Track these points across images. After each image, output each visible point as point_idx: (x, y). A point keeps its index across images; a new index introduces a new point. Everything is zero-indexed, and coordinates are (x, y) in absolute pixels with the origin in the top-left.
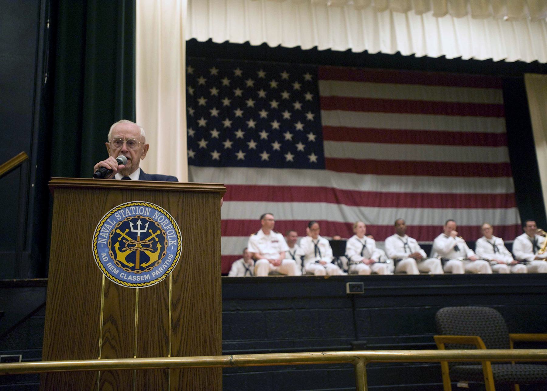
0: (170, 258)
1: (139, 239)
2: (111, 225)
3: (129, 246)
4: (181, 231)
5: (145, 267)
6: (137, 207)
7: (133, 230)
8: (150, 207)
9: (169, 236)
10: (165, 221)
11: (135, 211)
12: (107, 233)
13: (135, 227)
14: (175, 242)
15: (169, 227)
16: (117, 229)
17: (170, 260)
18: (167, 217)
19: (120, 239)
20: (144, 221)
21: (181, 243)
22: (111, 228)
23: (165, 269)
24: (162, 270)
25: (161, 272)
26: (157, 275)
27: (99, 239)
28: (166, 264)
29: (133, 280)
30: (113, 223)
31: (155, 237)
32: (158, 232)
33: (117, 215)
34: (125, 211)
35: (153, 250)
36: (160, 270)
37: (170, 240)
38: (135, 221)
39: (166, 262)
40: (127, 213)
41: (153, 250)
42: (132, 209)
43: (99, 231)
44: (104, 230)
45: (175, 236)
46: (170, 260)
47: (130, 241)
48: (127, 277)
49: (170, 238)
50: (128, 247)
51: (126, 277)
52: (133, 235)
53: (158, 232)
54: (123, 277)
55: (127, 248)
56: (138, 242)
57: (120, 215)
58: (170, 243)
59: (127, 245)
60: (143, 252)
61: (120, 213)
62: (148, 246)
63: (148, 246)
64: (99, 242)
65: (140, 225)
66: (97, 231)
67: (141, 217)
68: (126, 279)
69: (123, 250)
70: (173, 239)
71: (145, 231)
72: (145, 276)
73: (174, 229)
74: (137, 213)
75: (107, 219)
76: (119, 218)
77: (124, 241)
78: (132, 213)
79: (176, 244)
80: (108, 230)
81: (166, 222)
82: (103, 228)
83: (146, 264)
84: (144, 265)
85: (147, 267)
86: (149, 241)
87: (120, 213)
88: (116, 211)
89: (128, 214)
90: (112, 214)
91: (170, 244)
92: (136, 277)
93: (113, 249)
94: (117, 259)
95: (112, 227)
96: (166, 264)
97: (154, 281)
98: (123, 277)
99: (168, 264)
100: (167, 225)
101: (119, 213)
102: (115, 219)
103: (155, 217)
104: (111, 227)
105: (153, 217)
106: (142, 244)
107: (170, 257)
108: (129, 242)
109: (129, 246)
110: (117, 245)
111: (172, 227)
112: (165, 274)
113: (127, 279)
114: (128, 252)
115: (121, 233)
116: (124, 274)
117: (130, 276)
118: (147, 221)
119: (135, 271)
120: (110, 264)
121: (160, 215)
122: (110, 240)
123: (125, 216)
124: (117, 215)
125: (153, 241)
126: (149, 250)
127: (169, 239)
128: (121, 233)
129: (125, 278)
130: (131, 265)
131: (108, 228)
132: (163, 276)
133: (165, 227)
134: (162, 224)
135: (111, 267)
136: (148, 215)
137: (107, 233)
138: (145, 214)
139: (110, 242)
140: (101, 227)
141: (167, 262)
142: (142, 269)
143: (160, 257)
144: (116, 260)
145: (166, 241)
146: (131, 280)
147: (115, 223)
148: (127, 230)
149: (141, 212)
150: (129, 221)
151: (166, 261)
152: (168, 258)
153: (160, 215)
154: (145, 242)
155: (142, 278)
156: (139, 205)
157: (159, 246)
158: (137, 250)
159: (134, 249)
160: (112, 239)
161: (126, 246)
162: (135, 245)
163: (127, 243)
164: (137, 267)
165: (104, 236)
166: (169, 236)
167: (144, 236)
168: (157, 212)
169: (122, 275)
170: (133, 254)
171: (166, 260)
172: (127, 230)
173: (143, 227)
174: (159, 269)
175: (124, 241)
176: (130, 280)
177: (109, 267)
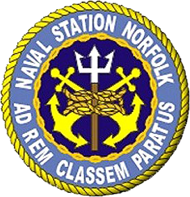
1: (95, 88)
7: (82, 70)
19: (59, 88)
31: (129, 84)
32: (136, 73)
52: (83, 80)
71: (107, 70)
84: (110, 142)
110: (54, 102)
130: (80, 142)
142: (105, 151)
148: (71, 70)
157: (137, 102)
164: (95, 148)
167: (106, 81)
172: (71, 70)
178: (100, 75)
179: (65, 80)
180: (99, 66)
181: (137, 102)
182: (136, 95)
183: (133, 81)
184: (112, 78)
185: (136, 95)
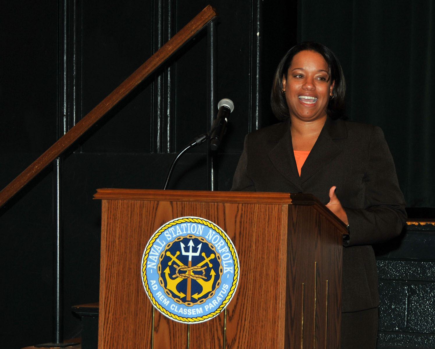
0: (225, 289)
1: (190, 264)
2: (161, 246)
3: (181, 272)
4: (238, 255)
5: (197, 299)
6: (189, 224)
7: (184, 253)
8: (203, 224)
9: (225, 261)
10: (220, 242)
11: (187, 230)
12: (156, 256)
13: (187, 249)
14: (231, 270)
15: (225, 250)
16: (167, 251)
17: (224, 291)
18: (222, 236)
19: (170, 263)
20: (197, 242)
21: (238, 270)
22: (161, 249)
23: (219, 302)
24: (216, 304)
25: (215, 305)
26: (210, 308)
27: (148, 263)
28: (220, 297)
29: (184, 313)
30: (163, 243)
31: (209, 263)
32: (212, 256)
33: (167, 234)
34: (175, 229)
35: (206, 278)
36: (214, 304)
37: (226, 267)
38: (186, 241)
39: (220, 294)
40: (178, 232)
41: (206, 278)
42: (183, 226)
43: (148, 253)
44: (153, 252)
45: (231, 261)
46: (224, 291)
47: (181, 266)
48: (178, 309)
49: (226, 264)
50: (179, 274)
51: (177, 310)
52: (184, 259)
53: (212, 256)
54: (173, 309)
55: (178, 275)
56: (189, 267)
57: (170, 234)
58: (226, 270)
59: (178, 271)
60: (195, 280)
61: (170, 232)
62: (200, 273)
63: (200, 273)
64: (148, 266)
65: (193, 246)
66: (146, 254)
67: (193, 237)
68: (177, 311)
69: (174, 276)
70: (229, 265)
71: (197, 254)
72: (197, 309)
73: (230, 253)
74: (189, 232)
75: (156, 239)
76: (169, 237)
77: (175, 266)
78: (184, 232)
79: (232, 272)
80: (158, 252)
81: (222, 243)
82: (152, 249)
83: (198, 294)
84: (196, 296)
85: (199, 299)
86: (202, 267)
87: (170, 232)
88: (165, 229)
89: (179, 233)
90: (162, 232)
91: (225, 272)
92: (187, 310)
93: (163, 275)
94: (167, 288)
95: (162, 249)
96: (220, 297)
97: (207, 315)
98: (173, 309)
99: (222, 296)
100: (222, 247)
101: (169, 232)
102: (165, 239)
103: (209, 237)
104: (161, 248)
105: (207, 237)
106: (193, 271)
107: (224, 287)
108: (180, 267)
109: (181, 272)
110: (167, 271)
111: (228, 250)
112: (219, 308)
113: (178, 311)
114: (179, 280)
115: (171, 256)
116: (175, 306)
117: (181, 309)
118: (200, 242)
119: (186, 303)
120: (160, 294)
121: (214, 235)
122: (160, 265)
123: (176, 236)
124: (167, 234)
125: (206, 267)
126: (202, 278)
127: (225, 265)
128: (171, 256)
129: (176, 310)
130: (182, 295)
131: (157, 249)
132: (216, 310)
133: (220, 249)
134: (216, 246)
135: (160, 296)
136: (201, 234)
137: (156, 256)
138: (198, 233)
139: (159, 267)
140: (150, 248)
141: (222, 294)
142: (194, 301)
143: (214, 287)
144: (166, 289)
145: (220, 267)
146: (182, 313)
147: (165, 243)
148: (178, 253)
149: (194, 230)
150: (180, 241)
151: (220, 293)
152: (223, 289)
153: (214, 235)
154: (197, 268)
155: (193, 312)
156: (191, 222)
157: (213, 273)
158: (188, 277)
159: (185, 277)
160: (162, 263)
161: (177, 272)
162: (186, 271)
163: (178, 269)
164: (189, 298)
165: (154, 259)
166: (225, 261)
167: (197, 260)
168: (211, 231)
169: (173, 307)
170: (185, 282)
171: (220, 292)
172: (178, 253)
173: (195, 250)
174: (213, 302)
175: (175, 266)
176: (180, 313)
177: (158, 297)
178: (193, 257)
179: (174, 258)
180: (193, 252)
181: (213, 273)
182: (212, 270)
183: (211, 261)
184: (200, 259)
185: (212, 270)
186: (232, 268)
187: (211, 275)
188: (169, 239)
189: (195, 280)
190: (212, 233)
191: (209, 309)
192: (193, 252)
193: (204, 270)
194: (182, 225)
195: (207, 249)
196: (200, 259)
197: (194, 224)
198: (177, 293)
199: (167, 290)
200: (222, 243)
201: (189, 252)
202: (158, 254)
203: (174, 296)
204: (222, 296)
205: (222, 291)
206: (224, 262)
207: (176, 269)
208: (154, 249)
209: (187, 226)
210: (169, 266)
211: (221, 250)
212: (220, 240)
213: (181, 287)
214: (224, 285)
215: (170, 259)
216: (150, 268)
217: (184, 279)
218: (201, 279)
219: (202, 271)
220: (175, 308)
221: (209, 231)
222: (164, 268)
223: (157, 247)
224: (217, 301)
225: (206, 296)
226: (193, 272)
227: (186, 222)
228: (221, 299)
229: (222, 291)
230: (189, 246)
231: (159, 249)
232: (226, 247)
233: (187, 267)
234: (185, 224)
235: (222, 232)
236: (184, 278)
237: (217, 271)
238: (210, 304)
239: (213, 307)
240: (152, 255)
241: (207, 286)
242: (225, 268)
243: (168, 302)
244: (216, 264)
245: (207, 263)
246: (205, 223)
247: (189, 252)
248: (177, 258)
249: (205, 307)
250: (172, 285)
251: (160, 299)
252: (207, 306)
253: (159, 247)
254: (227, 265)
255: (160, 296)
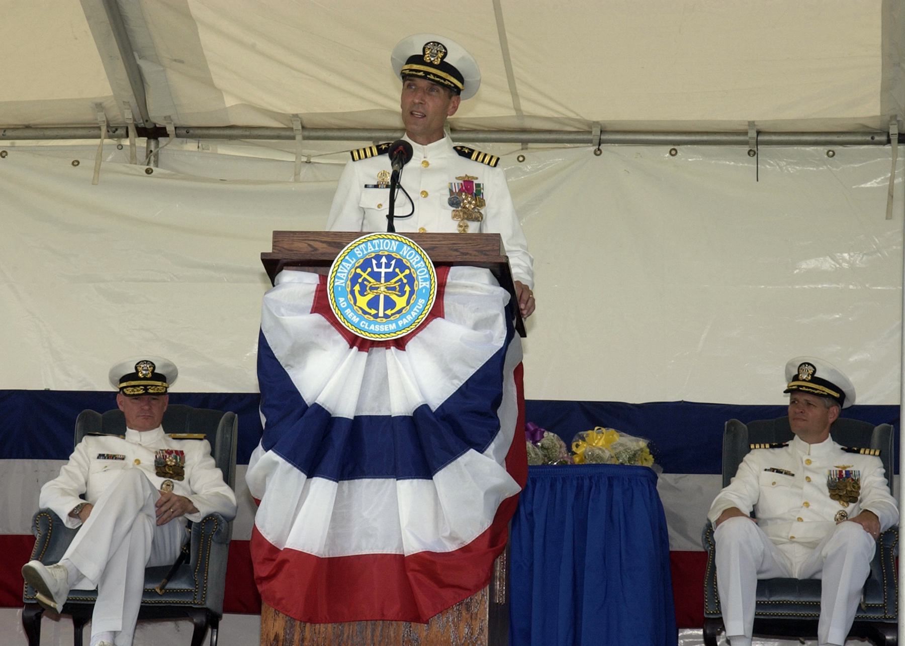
0: (421, 303)
1: (383, 280)
2: (350, 263)
3: (372, 288)
6: (381, 241)
7: (376, 269)
9: (421, 276)
10: (416, 257)
11: (379, 246)
12: (345, 273)
13: (379, 265)
14: (427, 284)
17: (420, 306)
19: (360, 280)
20: (389, 258)
27: (336, 280)
28: (415, 311)
30: (353, 260)
31: (403, 278)
33: (357, 251)
34: (367, 245)
35: (400, 294)
37: (422, 282)
38: (378, 257)
39: (415, 309)
40: (369, 248)
41: (400, 294)
44: (341, 269)
45: (427, 276)
46: (420, 306)
48: (369, 326)
49: (421, 279)
52: (376, 276)
55: (369, 291)
58: (422, 285)
62: (394, 289)
63: (394, 289)
64: (336, 284)
68: (367, 328)
70: (425, 280)
71: (391, 270)
76: (360, 254)
77: (365, 283)
79: (428, 286)
80: (346, 269)
81: (417, 259)
82: (341, 267)
84: (389, 312)
85: (393, 315)
90: (352, 249)
96: (415, 311)
98: (363, 326)
100: (417, 263)
101: (359, 248)
103: (403, 252)
107: (421, 302)
108: (371, 284)
109: (372, 288)
110: (357, 288)
111: (424, 265)
114: (370, 296)
115: (362, 273)
116: (365, 323)
117: (373, 325)
118: (394, 258)
121: (409, 251)
125: (400, 283)
127: (420, 280)
128: (362, 273)
129: (366, 327)
130: (373, 312)
131: (347, 267)
133: (416, 265)
135: (349, 314)
137: (345, 273)
138: (391, 249)
141: (417, 308)
143: (408, 302)
144: (356, 306)
148: (369, 270)
152: (418, 304)
153: (409, 251)
157: (407, 288)
159: (377, 293)
161: (368, 288)
162: (378, 288)
164: (381, 314)
165: (342, 277)
166: (421, 276)
167: (389, 277)
168: (405, 247)
169: (363, 324)
172: (369, 270)
175: (365, 283)
176: (372, 330)
177: (347, 314)
179: (365, 275)
180: (386, 268)
181: (407, 288)
184: (394, 274)
186: (428, 283)
187: (406, 291)
188: (359, 256)
189: (388, 296)
190: (407, 249)
191: (403, 324)
192: (386, 268)
193: (399, 285)
194: (374, 241)
195: (401, 265)
196: (394, 274)
197: (388, 241)
198: (367, 310)
199: (357, 307)
200: (417, 259)
201: (381, 268)
202: (346, 271)
203: (365, 312)
204: (418, 311)
205: (417, 306)
206: (420, 277)
207: (367, 286)
208: (343, 266)
209: (380, 242)
210: (360, 284)
211: (417, 265)
212: (415, 256)
213: (373, 303)
214: (420, 299)
215: (361, 276)
216: (338, 286)
217: (376, 296)
218: (395, 295)
219: (395, 287)
220: (365, 325)
221: (404, 247)
222: (353, 285)
223: (346, 264)
224: (412, 316)
225: (400, 311)
226: (386, 288)
227: (379, 238)
228: (416, 314)
229: (417, 306)
230: (382, 263)
231: (348, 266)
232: (422, 262)
233: (379, 283)
234: (377, 241)
235: (418, 247)
236: (375, 294)
237: (412, 286)
238: (404, 319)
239: (408, 322)
240: (340, 272)
241: (400, 302)
242: (420, 283)
243: (358, 319)
244: (411, 279)
245: (401, 278)
246: (399, 239)
247: (381, 268)
248: (368, 274)
249: (399, 322)
250: (362, 301)
251: (349, 316)
252: (401, 321)
253: (348, 264)
254: (422, 280)
255: (349, 314)
